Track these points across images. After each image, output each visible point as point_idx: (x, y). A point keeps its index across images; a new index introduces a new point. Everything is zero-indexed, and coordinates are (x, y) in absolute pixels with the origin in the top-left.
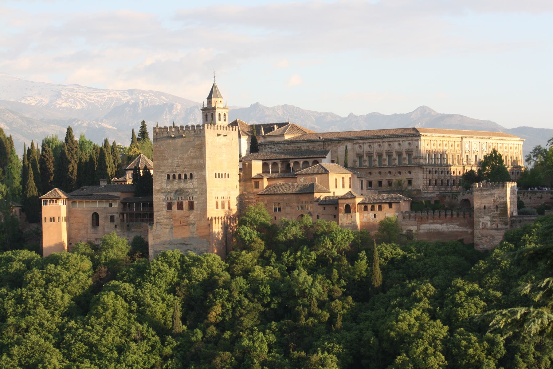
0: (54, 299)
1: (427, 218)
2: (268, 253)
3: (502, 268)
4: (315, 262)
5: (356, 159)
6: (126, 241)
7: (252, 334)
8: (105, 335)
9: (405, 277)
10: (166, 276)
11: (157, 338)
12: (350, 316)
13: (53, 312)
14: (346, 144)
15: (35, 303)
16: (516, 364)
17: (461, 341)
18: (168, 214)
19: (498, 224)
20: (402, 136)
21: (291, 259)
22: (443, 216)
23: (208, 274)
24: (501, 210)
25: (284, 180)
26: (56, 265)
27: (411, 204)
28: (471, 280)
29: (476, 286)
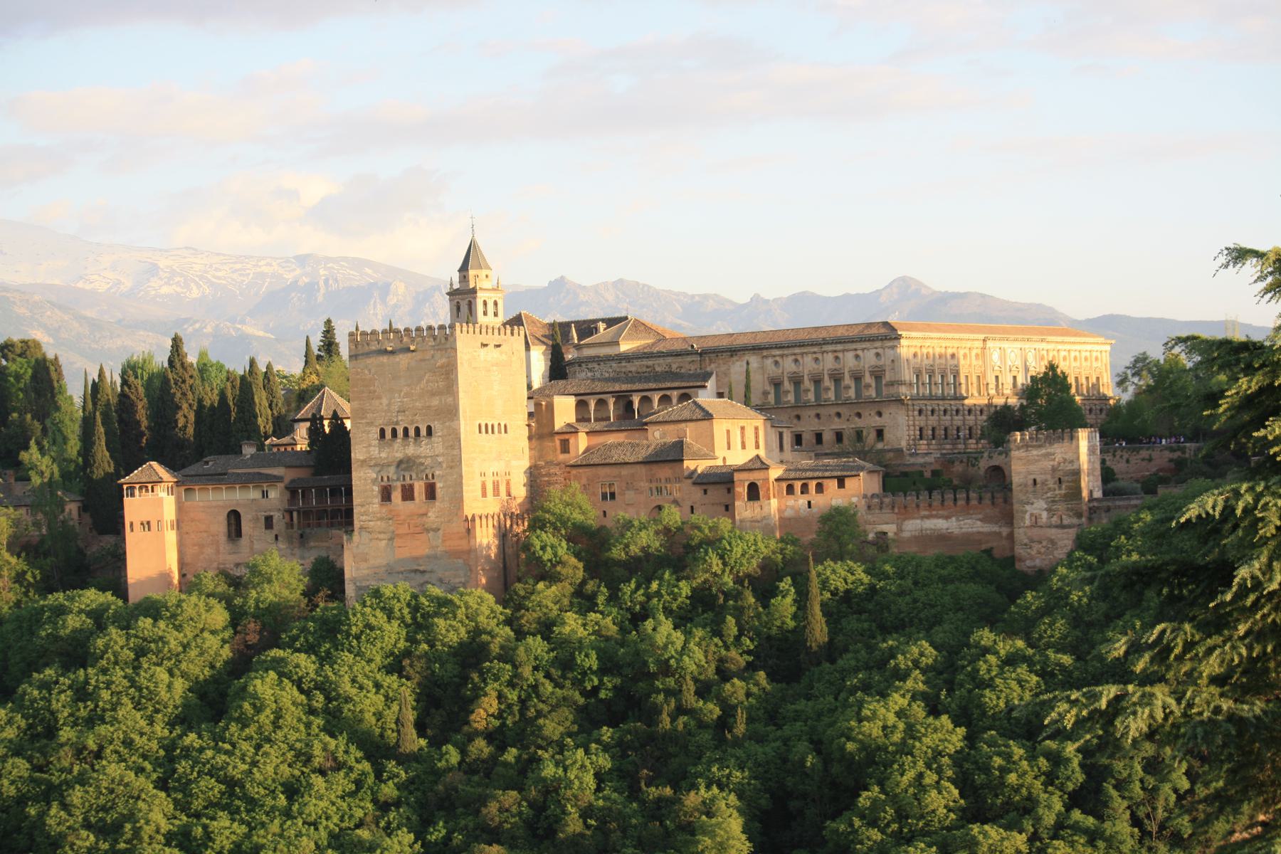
0: (152, 688)
1: (918, 506)
2: (590, 586)
3: (1071, 605)
4: (688, 602)
6: (298, 568)
7: (561, 753)
8: (258, 762)
9: (874, 628)
10: (382, 637)
11: (366, 766)
13: (151, 716)
14: (746, 358)
15: (115, 699)
16: (1107, 802)
17: (991, 758)
18: (384, 511)
19: (1064, 517)
20: (862, 340)
21: (640, 596)
22: (949, 503)
23: (468, 632)
26: (155, 620)
28: (1011, 633)
29: (1020, 644)
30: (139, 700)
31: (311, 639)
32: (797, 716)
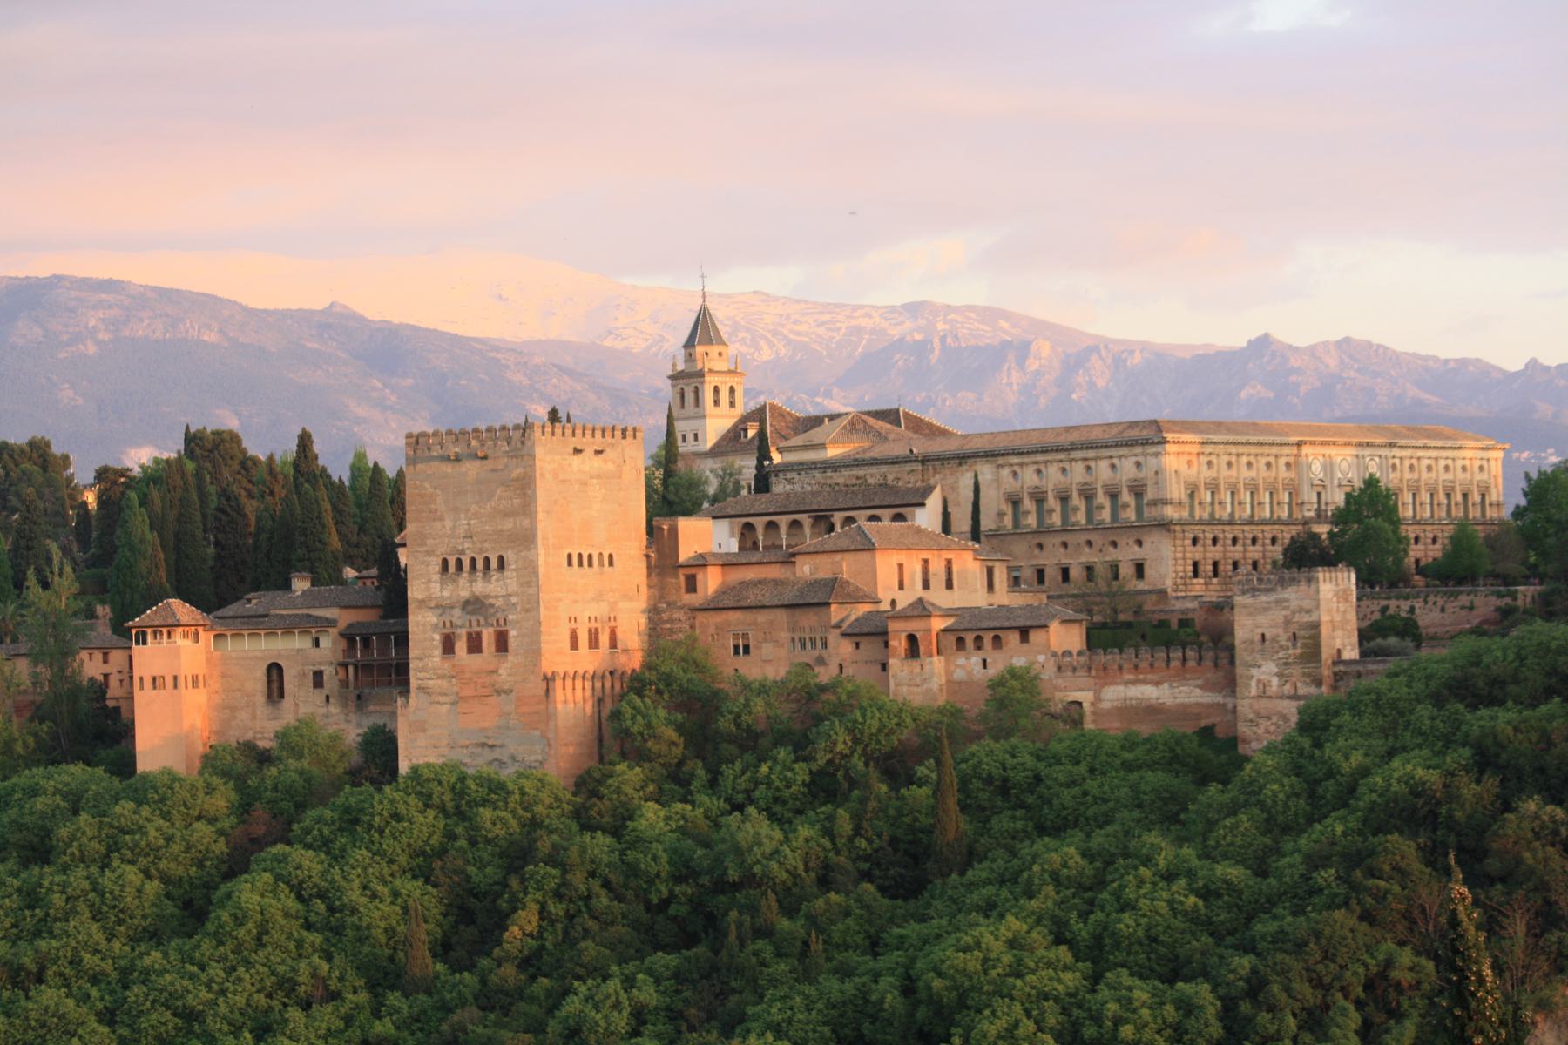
0: (117, 893)
1: (1120, 668)
11: (363, 997)
12: (861, 936)
18: (446, 665)
19: (1299, 685)
21: (743, 782)
23: (524, 826)
24: (1304, 645)
26: (139, 804)
27: (1088, 629)
30: (100, 908)
31: (326, 832)
32: (901, 943)
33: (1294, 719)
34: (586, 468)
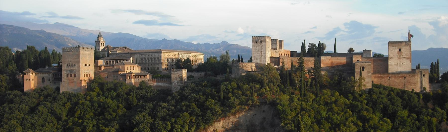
5: (140, 60)
25: (112, 67)
33: (179, 88)
34: (86, 53)
